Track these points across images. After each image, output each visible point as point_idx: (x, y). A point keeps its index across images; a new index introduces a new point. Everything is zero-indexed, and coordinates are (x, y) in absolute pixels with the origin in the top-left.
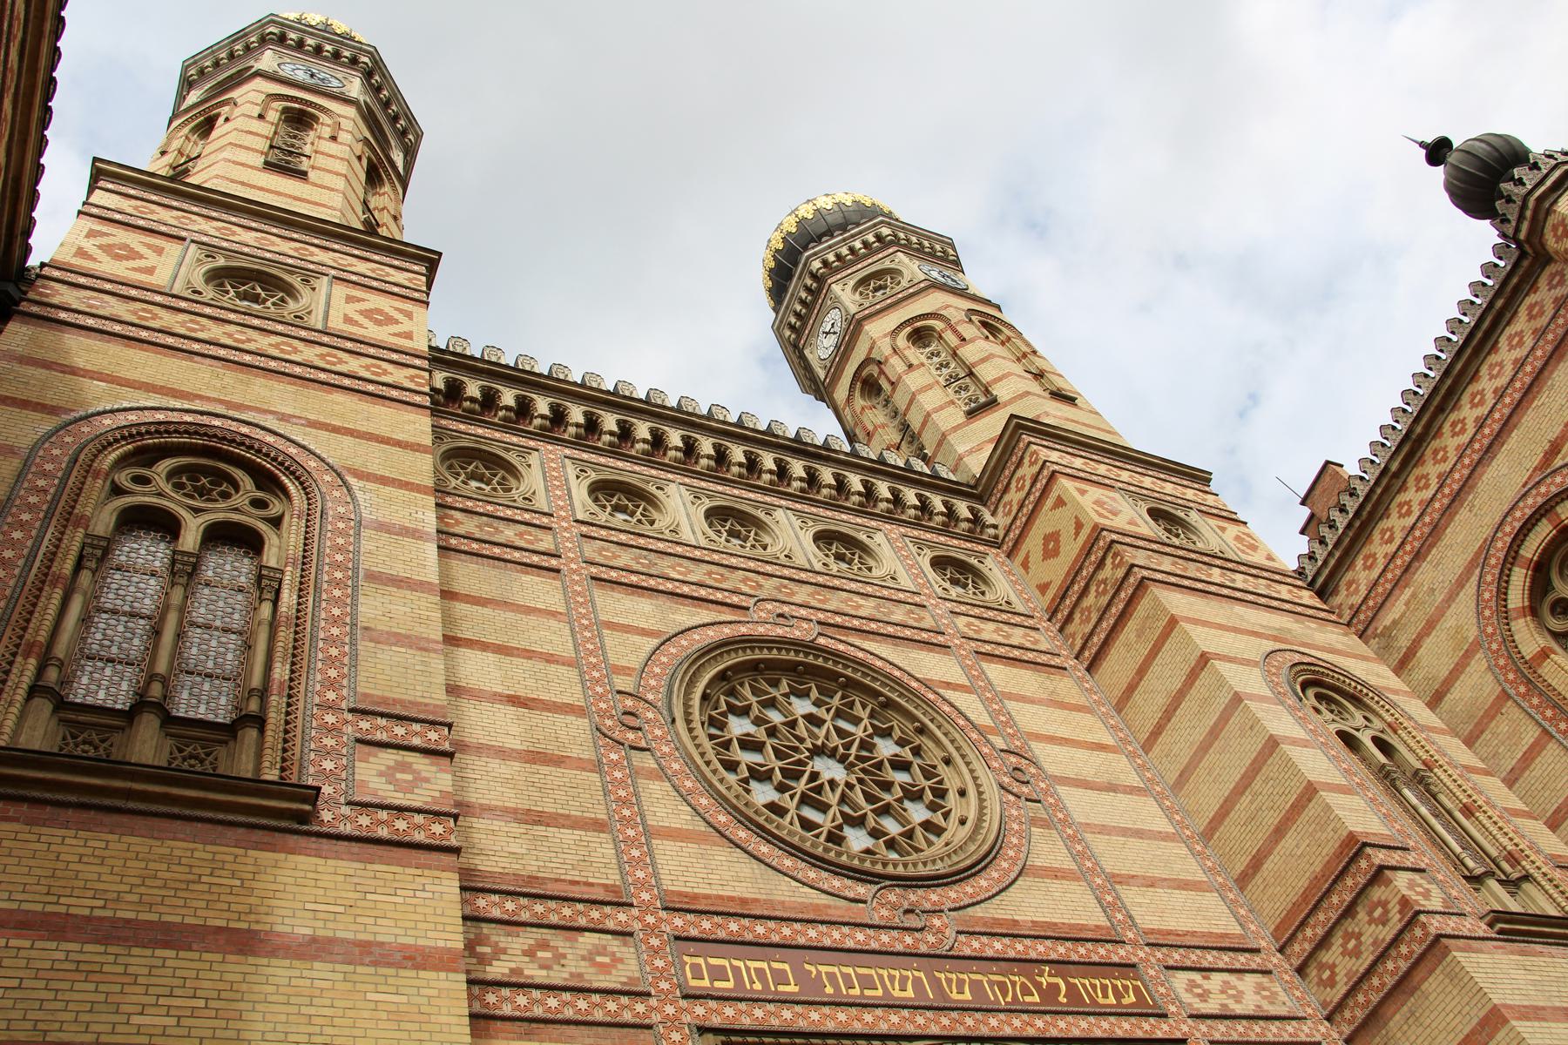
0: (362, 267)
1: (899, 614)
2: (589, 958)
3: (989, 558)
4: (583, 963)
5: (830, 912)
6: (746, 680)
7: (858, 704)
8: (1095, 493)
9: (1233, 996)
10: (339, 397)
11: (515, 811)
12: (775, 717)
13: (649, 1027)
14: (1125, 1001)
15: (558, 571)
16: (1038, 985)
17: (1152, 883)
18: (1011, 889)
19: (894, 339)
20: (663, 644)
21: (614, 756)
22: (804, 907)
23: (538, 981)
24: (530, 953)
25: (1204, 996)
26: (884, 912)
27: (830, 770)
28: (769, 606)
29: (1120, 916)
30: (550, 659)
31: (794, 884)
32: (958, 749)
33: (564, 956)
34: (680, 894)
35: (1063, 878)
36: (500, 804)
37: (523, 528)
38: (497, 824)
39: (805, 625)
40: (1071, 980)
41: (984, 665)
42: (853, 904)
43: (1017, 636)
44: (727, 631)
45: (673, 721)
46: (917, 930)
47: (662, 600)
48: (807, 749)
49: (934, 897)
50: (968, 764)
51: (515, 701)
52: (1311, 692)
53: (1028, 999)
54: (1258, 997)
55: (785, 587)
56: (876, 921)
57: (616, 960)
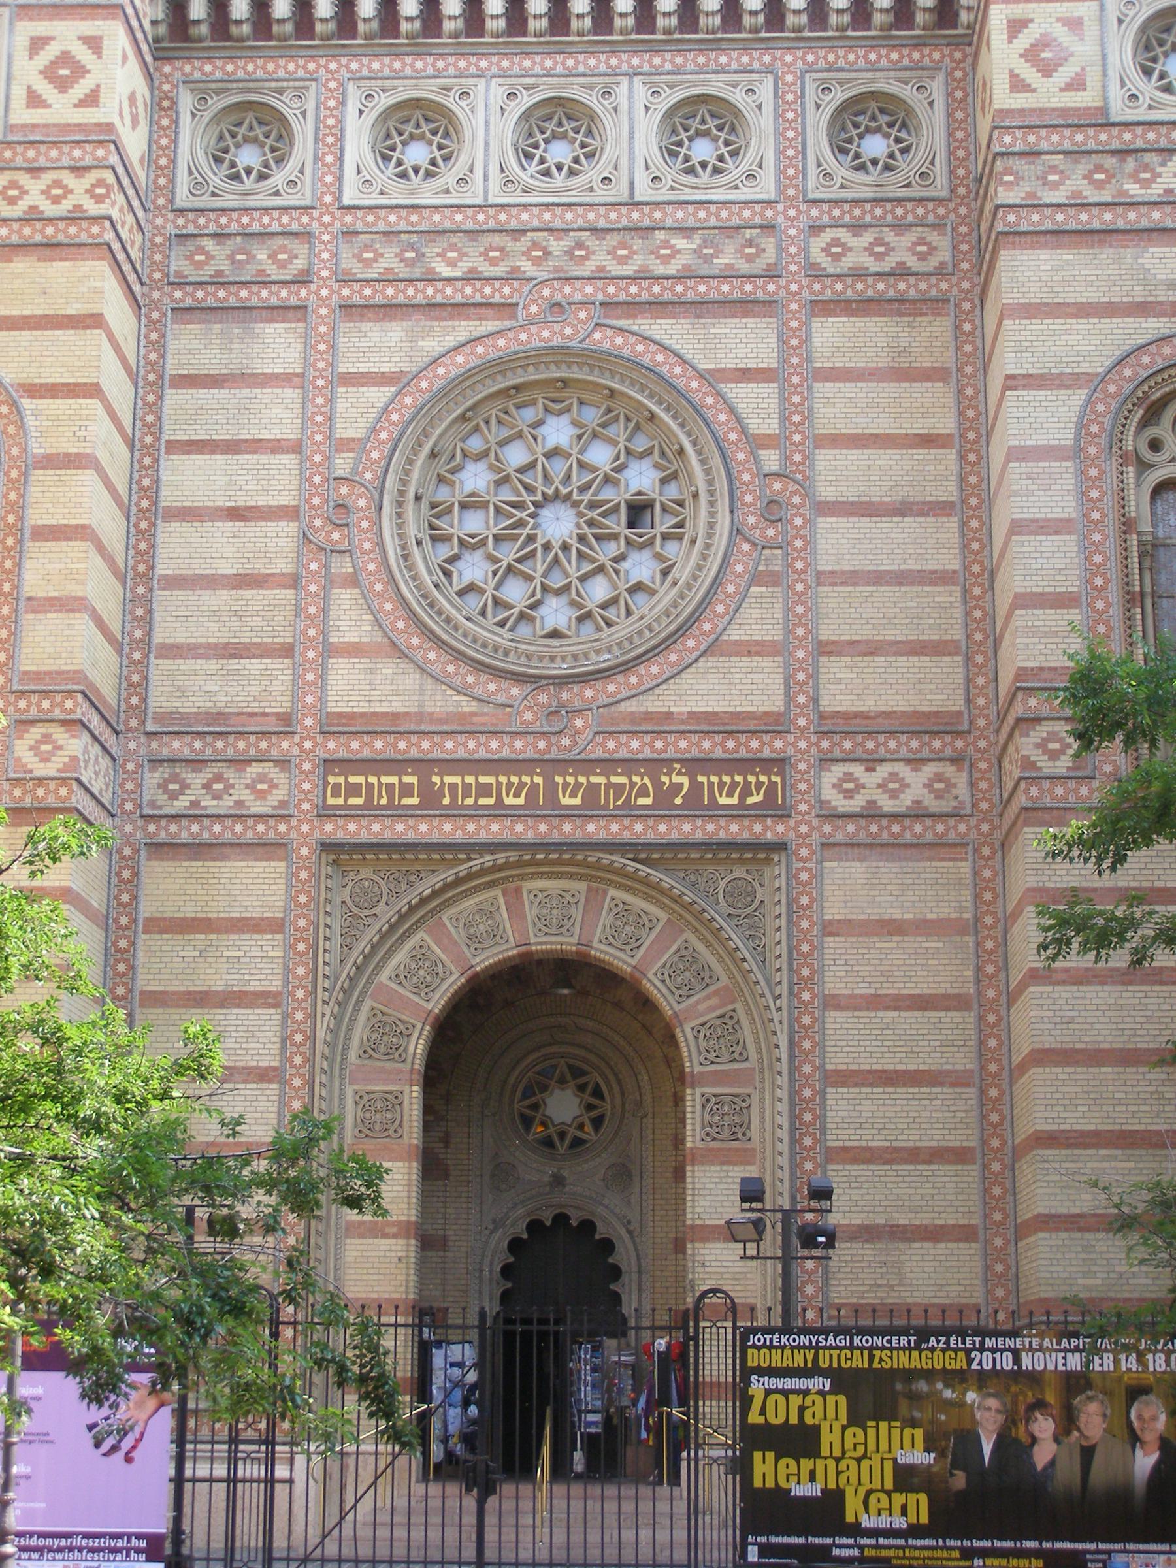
2: (251, 787)
4: (248, 791)
5: (475, 719)
6: (494, 411)
7: (622, 416)
9: (893, 790)
12: (516, 456)
13: (285, 845)
14: (750, 800)
15: (302, 309)
16: (657, 784)
17: (872, 649)
18: (683, 675)
20: (399, 392)
21: (314, 566)
23: (209, 812)
24: (207, 786)
25: (849, 794)
26: (528, 716)
28: (546, 292)
30: (276, 447)
31: (450, 692)
32: (710, 483)
33: (232, 786)
34: (340, 715)
35: (758, 654)
36: (203, 640)
37: (280, 241)
39: (582, 315)
40: (702, 779)
41: (817, 323)
42: (500, 711)
46: (554, 734)
47: (419, 322)
49: (589, 693)
50: (712, 504)
51: (236, 514)
53: (642, 801)
54: (926, 791)
55: (580, 245)
56: (517, 726)
57: (273, 786)
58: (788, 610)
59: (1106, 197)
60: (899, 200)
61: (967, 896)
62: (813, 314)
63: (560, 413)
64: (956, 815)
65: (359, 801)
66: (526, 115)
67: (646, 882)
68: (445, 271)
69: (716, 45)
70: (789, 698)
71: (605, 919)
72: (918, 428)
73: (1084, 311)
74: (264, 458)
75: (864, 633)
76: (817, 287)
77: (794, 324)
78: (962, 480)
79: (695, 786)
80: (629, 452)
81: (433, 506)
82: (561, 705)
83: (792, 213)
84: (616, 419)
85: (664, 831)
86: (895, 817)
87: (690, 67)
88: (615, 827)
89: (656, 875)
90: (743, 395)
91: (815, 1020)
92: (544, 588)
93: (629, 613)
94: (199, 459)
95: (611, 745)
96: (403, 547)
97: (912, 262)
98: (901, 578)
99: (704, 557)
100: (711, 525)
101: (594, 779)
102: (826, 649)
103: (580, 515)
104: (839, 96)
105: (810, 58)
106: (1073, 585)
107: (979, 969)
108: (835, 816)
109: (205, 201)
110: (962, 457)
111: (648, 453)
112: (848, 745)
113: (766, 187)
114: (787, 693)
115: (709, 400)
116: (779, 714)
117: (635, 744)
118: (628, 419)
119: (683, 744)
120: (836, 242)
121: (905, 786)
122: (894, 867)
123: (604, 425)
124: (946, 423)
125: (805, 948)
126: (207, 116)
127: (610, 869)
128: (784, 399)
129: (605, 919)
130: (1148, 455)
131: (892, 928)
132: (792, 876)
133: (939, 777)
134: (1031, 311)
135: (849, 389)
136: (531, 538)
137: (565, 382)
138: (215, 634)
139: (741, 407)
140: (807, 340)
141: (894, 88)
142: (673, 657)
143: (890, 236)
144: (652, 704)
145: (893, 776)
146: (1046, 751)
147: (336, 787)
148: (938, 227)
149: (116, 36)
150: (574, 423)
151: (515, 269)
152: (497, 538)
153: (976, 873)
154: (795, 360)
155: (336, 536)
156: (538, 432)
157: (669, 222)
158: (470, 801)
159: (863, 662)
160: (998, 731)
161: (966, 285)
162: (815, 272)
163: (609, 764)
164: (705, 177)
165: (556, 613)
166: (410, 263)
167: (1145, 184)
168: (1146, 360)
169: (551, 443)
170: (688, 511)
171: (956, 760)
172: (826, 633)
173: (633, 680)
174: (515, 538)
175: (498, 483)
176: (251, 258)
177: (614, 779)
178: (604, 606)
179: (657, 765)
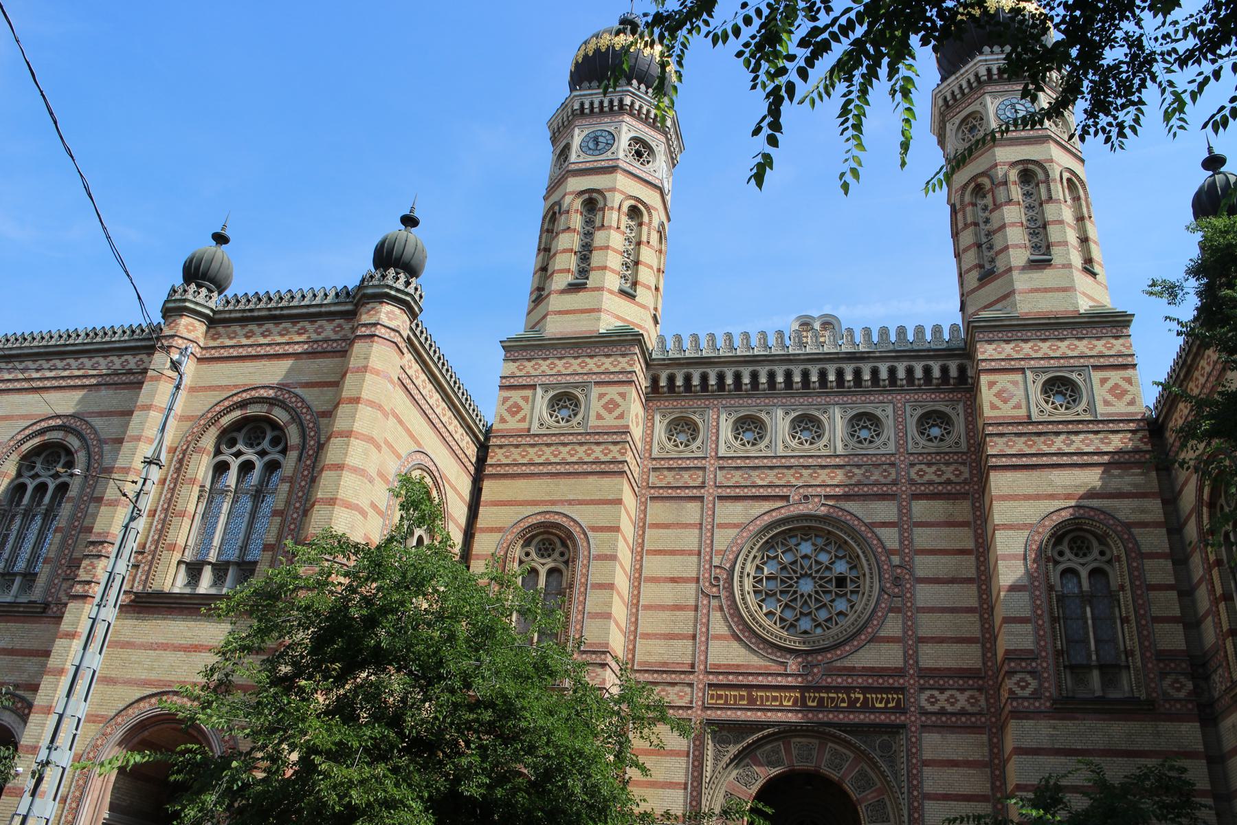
0: (608, 364)
1: (876, 476)
3: (961, 404)
8: (1003, 380)
10: (591, 479)
11: (664, 634)
16: (849, 698)
17: (941, 640)
19: (963, 195)
22: (760, 667)
25: (933, 704)
27: (807, 587)
28: (801, 491)
29: (911, 662)
32: (871, 569)
38: (658, 641)
40: (868, 696)
41: (914, 503)
43: (949, 473)
44: (776, 515)
45: (733, 579)
48: (797, 578)
49: (820, 658)
50: (872, 578)
51: (673, 580)
52: (1066, 541)
58: (904, 623)
59: (1033, 451)
60: (947, 453)
61: (986, 750)
62: (913, 499)
63: (806, 540)
64: (980, 714)
65: (722, 702)
66: (793, 421)
67: (844, 740)
68: (760, 483)
69: (869, 393)
70: (906, 662)
71: (827, 756)
72: (958, 546)
73: (1027, 497)
74: (685, 557)
75: (938, 633)
76: (913, 488)
77: (904, 503)
78: (978, 568)
79: (866, 699)
80: (836, 556)
81: (754, 578)
82: (808, 662)
83: (902, 458)
84: (830, 543)
85: (853, 718)
86: (953, 714)
87: (859, 401)
88: (831, 716)
89: (849, 737)
90: (884, 533)
91: (919, 804)
92: (801, 613)
93: (837, 624)
94: (659, 557)
95: (829, 680)
96: (742, 595)
97: (953, 478)
98: (953, 610)
99: (868, 601)
100: (871, 587)
101: (822, 695)
102: (922, 640)
103: (816, 582)
104: (920, 412)
105: (908, 397)
106: (1027, 613)
107: (993, 784)
108: (925, 713)
109: (664, 455)
110: (977, 559)
111: (844, 557)
112: (931, 682)
113: (892, 448)
114: (904, 659)
115: (869, 535)
116: (902, 668)
117: (839, 680)
118: (836, 543)
119: (860, 680)
120: (921, 470)
121: (957, 700)
122: (954, 736)
123: (825, 545)
124: (970, 545)
125: (915, 771)
126: (666, 422)
127: (829, 734)
128: (901, 534)
129: (827, 756)
130: (1058, 558)
131: (953, 764)
132: (908, 739)
133: (972, 697)
134: (1004, 498)
135: (928, 530)
136: (795, 592)
137: (809, 527)
138: (663, 629)
139: (883, 538)
140: (910, 510)
141: (943, 409)
142: (855, 643)
143: (944, 468)
144: (847, 663)
145: (952, 696)
146: (1019, 686)
147: (712, 695)
148: (964, 464)
149: (633, 393)
150: (813, 544)
151: (789, 482)
152: (782, 592)
153: (990, 740)
154: (905, 519)
155: (714, 589)
156: (798, 548)
157: (851, 463)
158: (768, 703)
159: (937, 646)
160: (997, 677)
161: (976, 487)
162: (912, 482)
163: (828, 689)
164: (866, 444)
165: (805, 624)
166: (746, 479)
167: (1050, 446)
168: (1054, 518)
169: (804, 553)
170: (861, 582)
171: (980, 690)
172: (921, 633)
173: (839, 652)
174: (788, 592)
175: (782, 569)
176: (682, 477)
177: (831, 695)
178: (826, 621)
179: (848, 689)
